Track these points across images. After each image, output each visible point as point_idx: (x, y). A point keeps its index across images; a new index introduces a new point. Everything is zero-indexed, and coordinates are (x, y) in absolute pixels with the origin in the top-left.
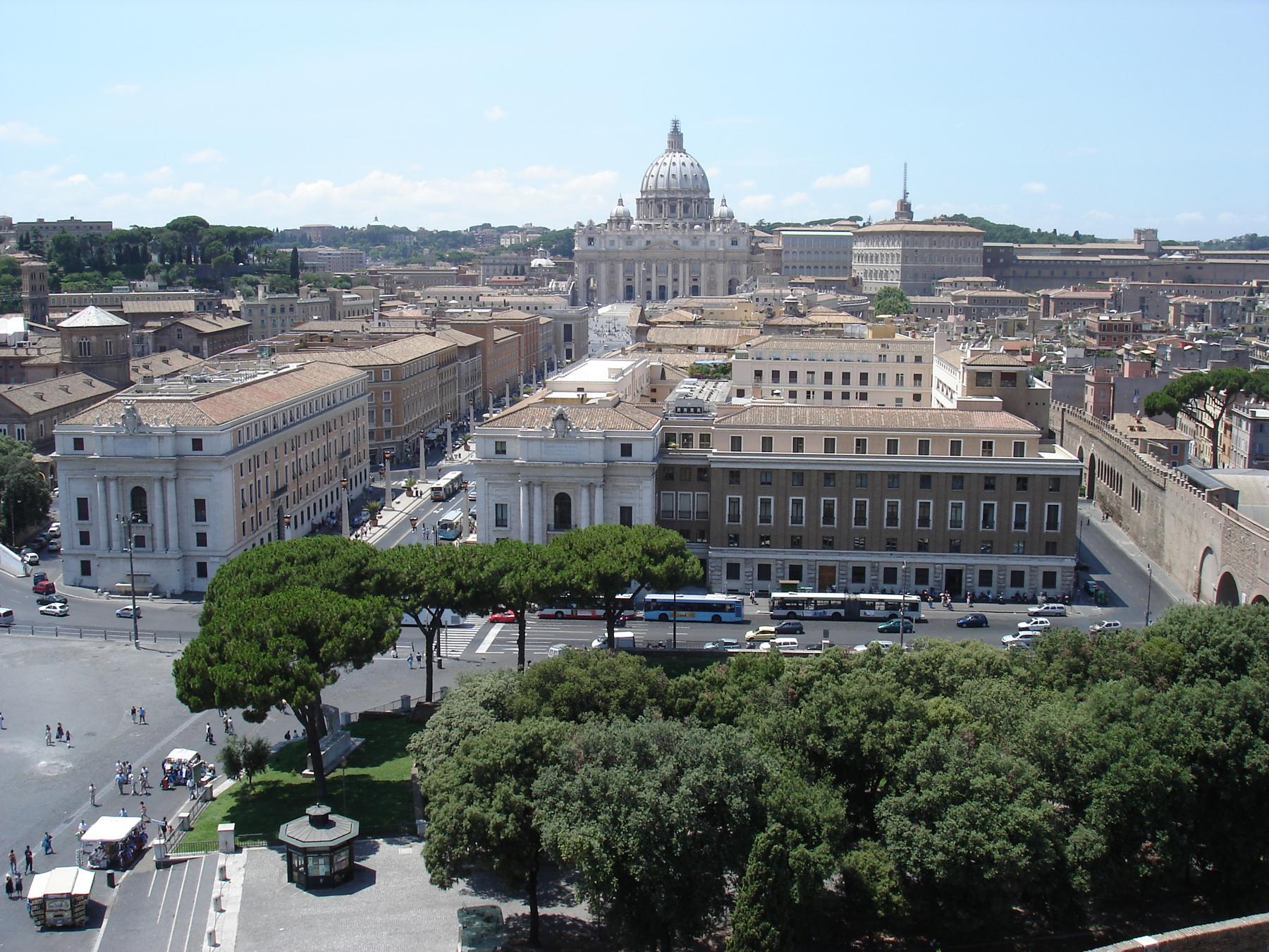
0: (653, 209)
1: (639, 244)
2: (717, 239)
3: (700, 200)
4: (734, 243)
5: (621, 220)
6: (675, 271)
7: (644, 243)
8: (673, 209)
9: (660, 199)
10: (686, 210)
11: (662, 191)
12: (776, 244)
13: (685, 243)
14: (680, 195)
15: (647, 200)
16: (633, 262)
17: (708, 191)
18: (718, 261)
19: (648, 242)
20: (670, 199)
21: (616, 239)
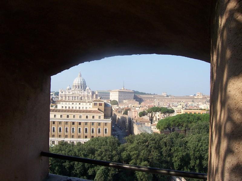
7: (72, 93)
8: (79, 87)
10: (81, 87)
12: (97, 93)
18: (86, 97)
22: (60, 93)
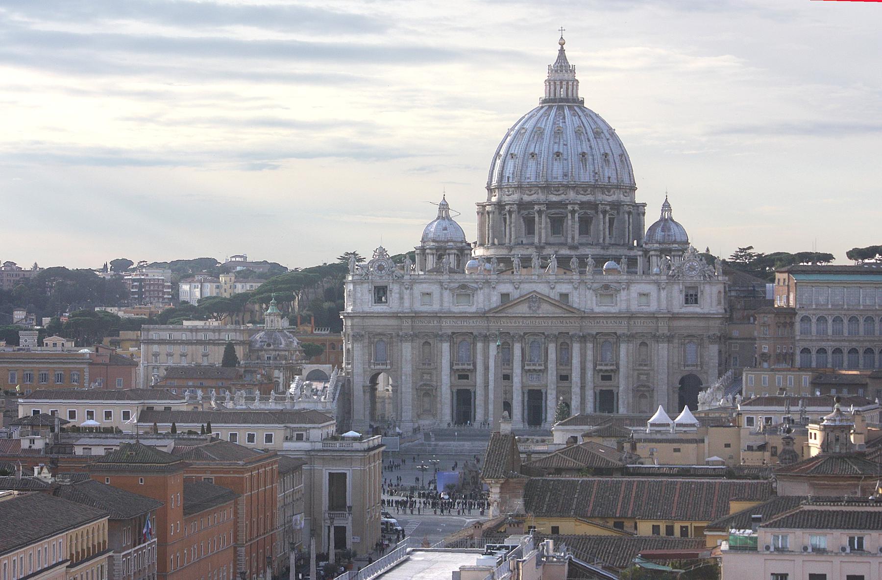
0: (514, 227)
1: (485, 300)
2: (651, 289)
3: (616, 206)
4: (691, 298)
5: (444, 249)
6: (564, 360)
7: (495, 300)
9: (531, 204)
10: (585, 224)
11: (531, 187)
13: (584, 299)
14: (572, 195)
15: (500, 205)
16: (472, 337)
17: (633, 188)
18: (656, 338)
19: (505, 296)
20: (550, 205)
21: (435, 289)
22: (356, 300)
